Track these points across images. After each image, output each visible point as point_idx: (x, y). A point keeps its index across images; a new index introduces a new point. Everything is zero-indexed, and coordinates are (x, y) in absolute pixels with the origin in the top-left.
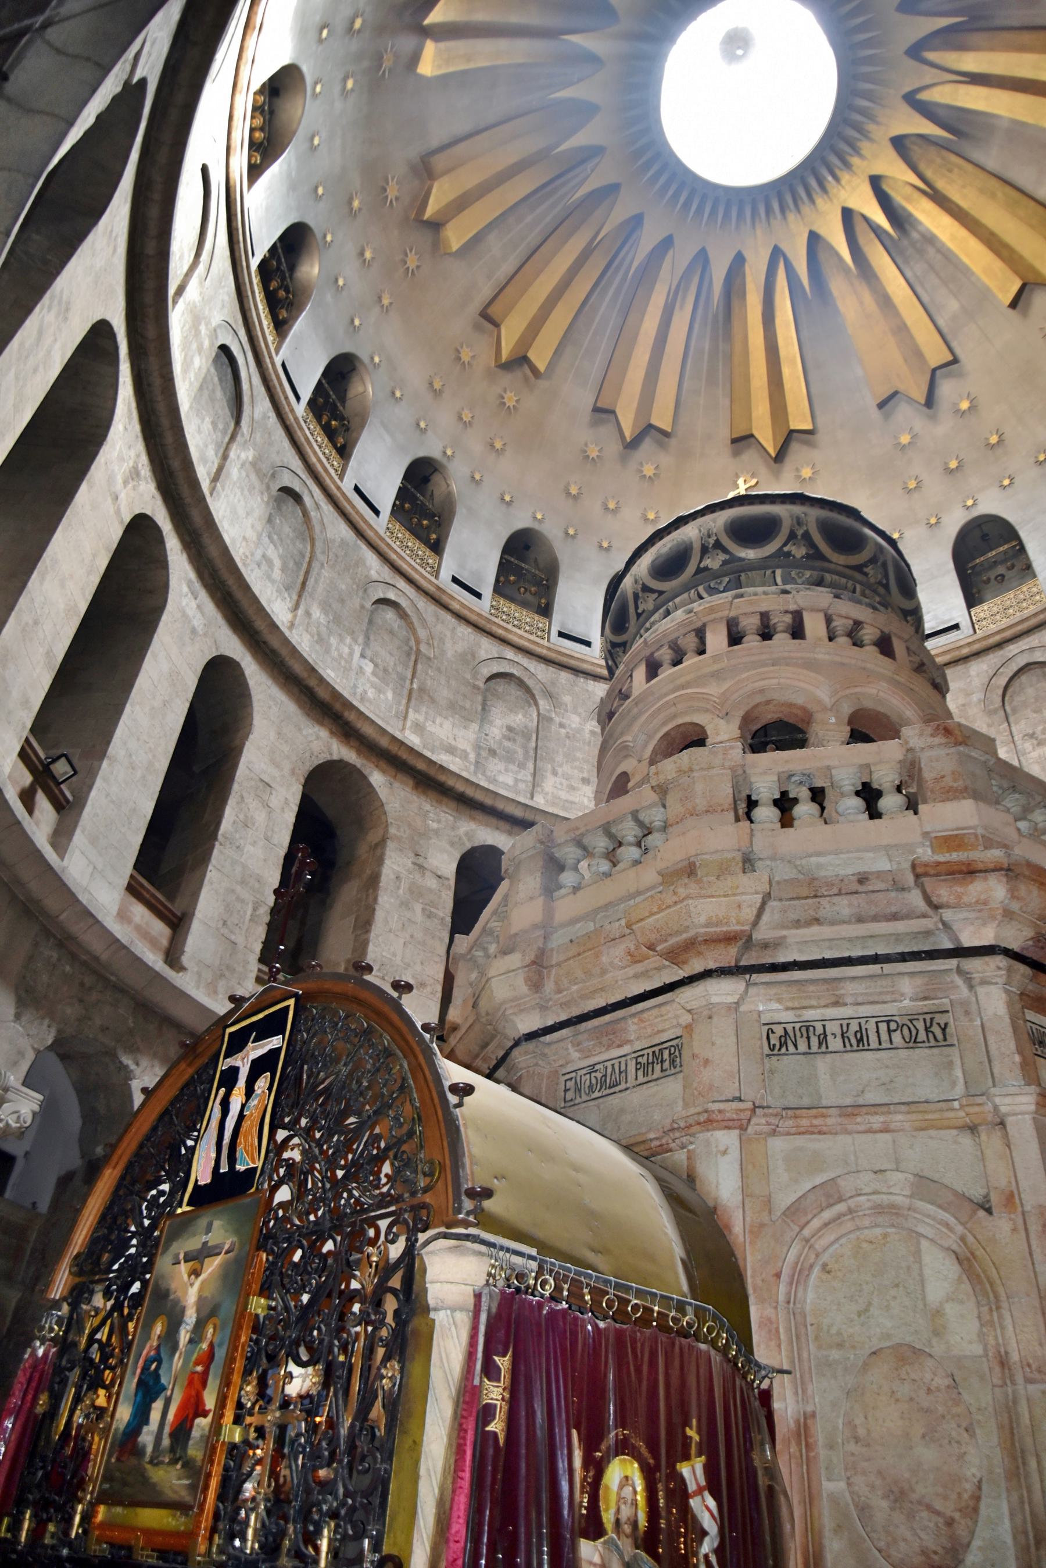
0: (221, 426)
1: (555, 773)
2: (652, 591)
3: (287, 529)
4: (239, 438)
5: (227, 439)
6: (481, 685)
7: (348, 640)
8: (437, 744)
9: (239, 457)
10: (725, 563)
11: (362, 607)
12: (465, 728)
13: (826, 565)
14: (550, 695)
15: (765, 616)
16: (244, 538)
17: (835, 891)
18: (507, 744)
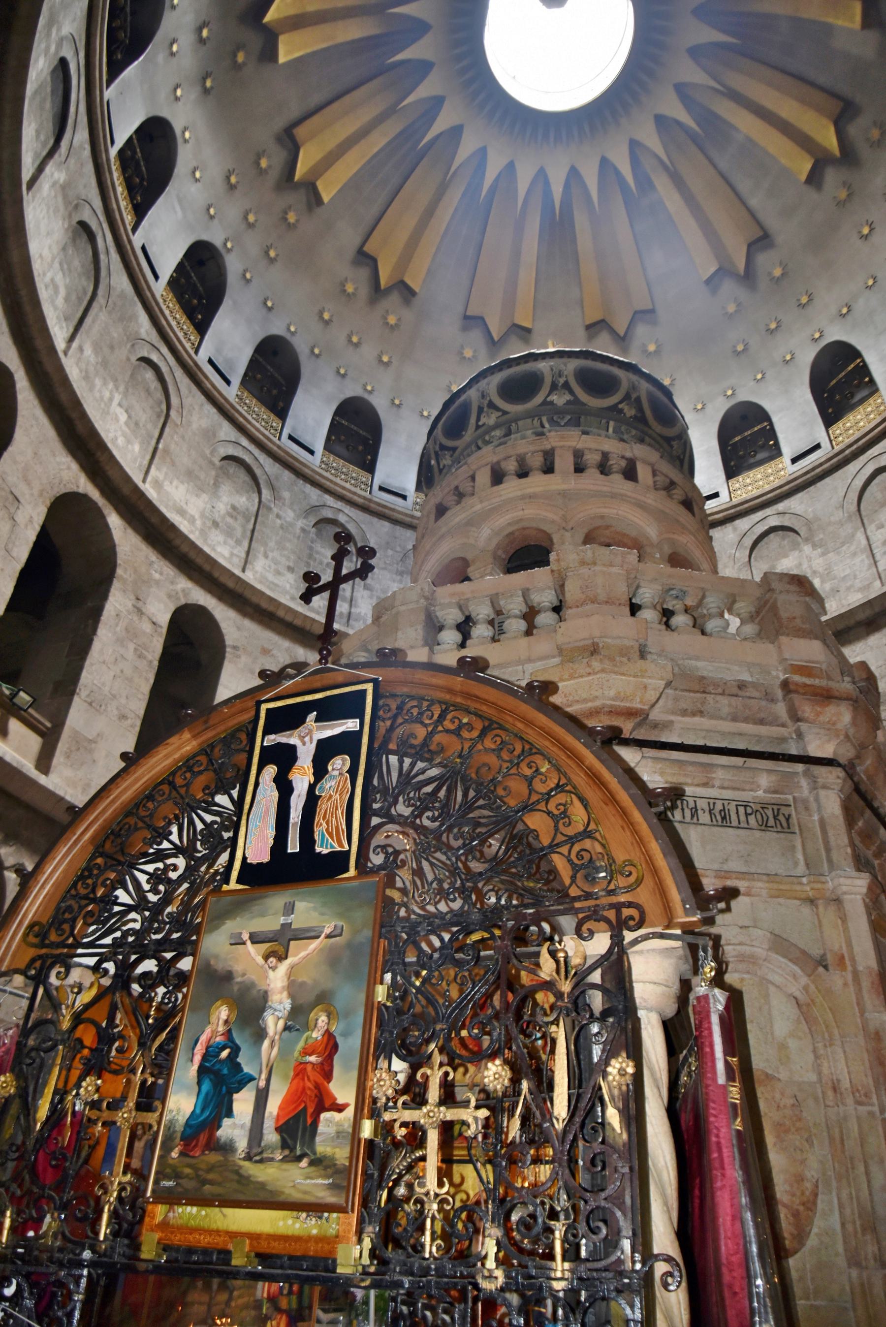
0: (42, 137)
1: (266, 556)
2: (497, 409)
3: (76, 263)
4: (56, 156)
5: (44, 153)
6: (216, 460)
7: (111, 386)
8: (171, 503)
9: (52, 175)
10: (568, 402)
11: (128, 359)
12: (197, 496)
13: (646, 429)
14: (273, 488)
15: (605, 456)
16: (41, 256)
17: (720, 690)
18: (229, 520)
